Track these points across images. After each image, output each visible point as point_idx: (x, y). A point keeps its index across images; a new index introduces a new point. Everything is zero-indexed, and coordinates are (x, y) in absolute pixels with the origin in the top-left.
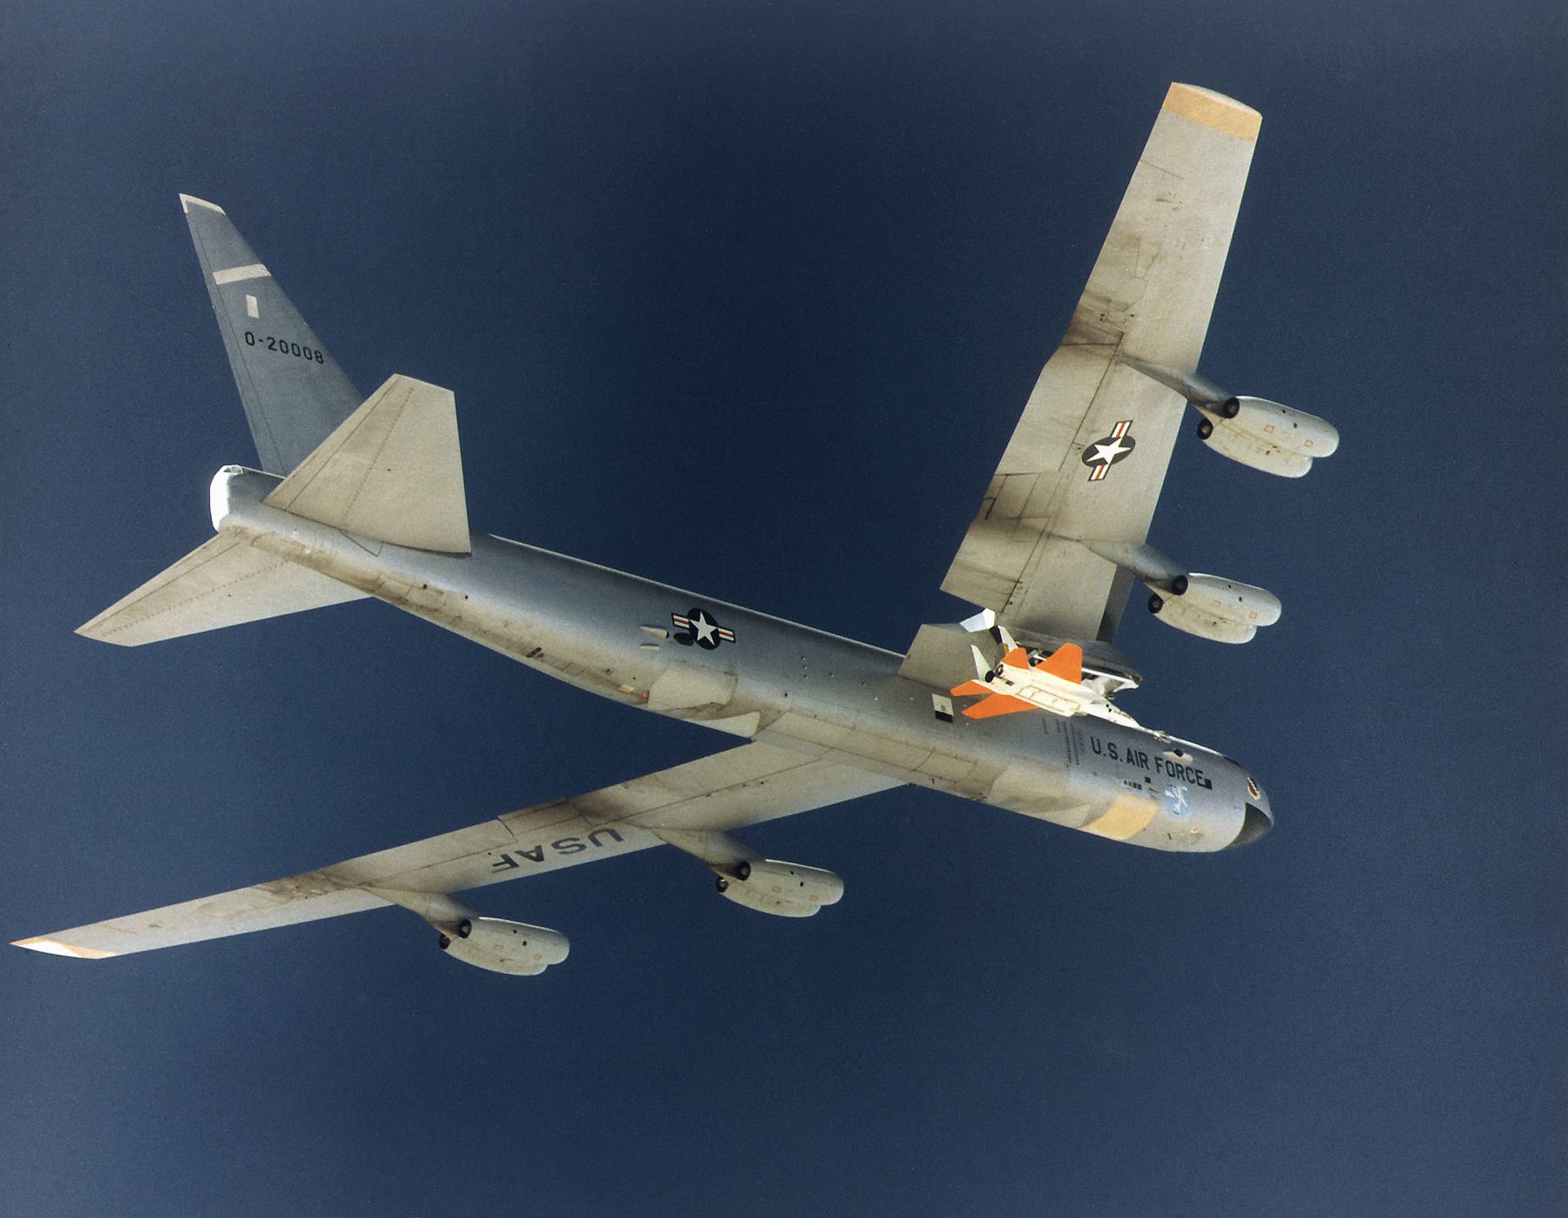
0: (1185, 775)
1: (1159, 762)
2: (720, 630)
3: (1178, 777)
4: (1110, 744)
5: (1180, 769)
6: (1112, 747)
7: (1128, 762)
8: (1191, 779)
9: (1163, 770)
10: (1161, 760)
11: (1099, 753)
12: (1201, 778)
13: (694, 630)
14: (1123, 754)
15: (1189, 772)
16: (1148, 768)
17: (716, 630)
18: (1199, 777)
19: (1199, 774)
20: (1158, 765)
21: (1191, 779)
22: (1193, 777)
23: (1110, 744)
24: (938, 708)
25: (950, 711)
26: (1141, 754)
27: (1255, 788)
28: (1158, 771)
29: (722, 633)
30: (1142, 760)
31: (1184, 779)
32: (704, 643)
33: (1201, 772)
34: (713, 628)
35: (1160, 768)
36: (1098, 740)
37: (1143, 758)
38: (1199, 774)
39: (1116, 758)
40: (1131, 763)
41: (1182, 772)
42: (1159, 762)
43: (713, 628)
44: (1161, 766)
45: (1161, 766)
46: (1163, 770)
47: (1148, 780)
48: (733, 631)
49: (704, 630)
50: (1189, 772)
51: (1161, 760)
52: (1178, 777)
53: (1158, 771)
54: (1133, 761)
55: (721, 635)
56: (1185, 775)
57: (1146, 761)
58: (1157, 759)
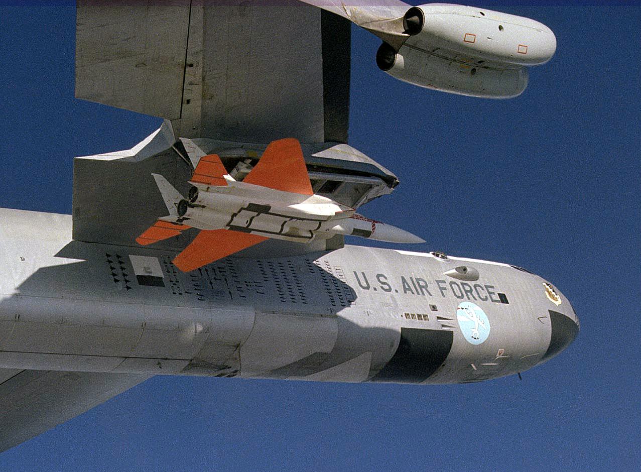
0: (474, 293)
1: (442, 285)
4: (378, 276)
7: (405, 292)
8: (483, 296)
9: (449, 293)
10: (444, 282)
11: (368, 288)
12: (494, 293)
14: (394, 282)
19: (491, 290)
20: (442, 289)
22: (484, 294)
23: (378, 276)
24: (139, 271)
25: (157, 271)
26: (417, 280)
27: (553, 293)
30: (421, 287)
33: (492, 287)
37: (422, 283)
38: (491, 290)
39: (390, 290)
41: (471, 291)
42: (442, 285)
45: (445, 289)
46: (449, 293)
47: (434, 308)
54: (410, 289)
56: (474, 293)
57: (426, 287)
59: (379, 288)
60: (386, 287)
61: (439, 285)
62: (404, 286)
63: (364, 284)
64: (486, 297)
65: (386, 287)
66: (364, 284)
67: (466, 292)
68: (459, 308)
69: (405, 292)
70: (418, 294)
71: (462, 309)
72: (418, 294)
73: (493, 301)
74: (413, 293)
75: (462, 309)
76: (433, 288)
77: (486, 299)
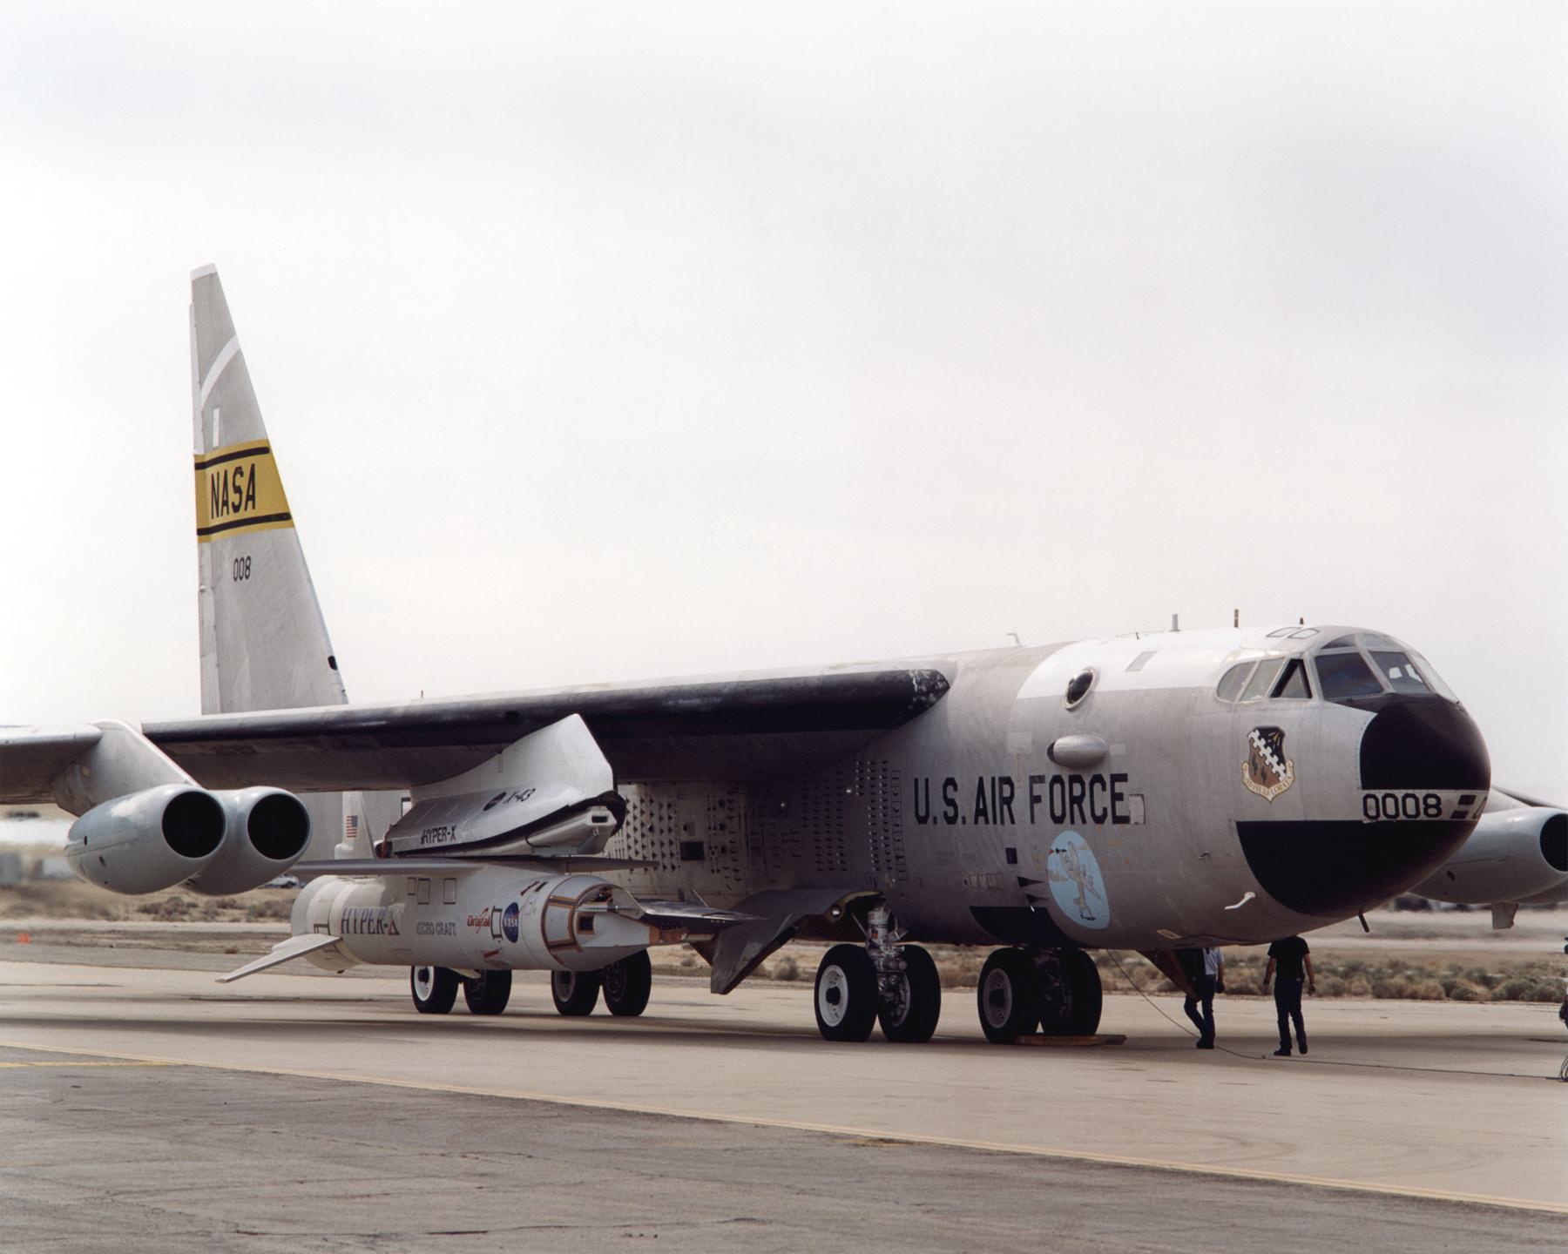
3: (1072, 822)
7: (976, 822)
8: (1099, 812)
10: (1041, 779)
15: (1097, 786)
16: (1013, 822)
18: (1117, 797)
19: (1119, 787)
20: (1036, 799)
21: (1099, 812)
22: (1103, 799)
31: (1084, 821)
33: (1123, 778)
35: (1037, 806)
39: (951, 820)
40: (981, 819)
41: (1077, 800)
46: (1042, 809)
50: (1097, 786)
52: (1072, 822)
57: (1008, 801)
59: (941, 819)
64: (1105, 810)
65: (951, 813)
66: (922, 813)
68: (1051, 852)
69: (976, 822)
70: (995, 822)
72: (995, 822)
74: (987, 821)
75: (1058, 851)
76: (1021, 803)
77: (1099, 820)
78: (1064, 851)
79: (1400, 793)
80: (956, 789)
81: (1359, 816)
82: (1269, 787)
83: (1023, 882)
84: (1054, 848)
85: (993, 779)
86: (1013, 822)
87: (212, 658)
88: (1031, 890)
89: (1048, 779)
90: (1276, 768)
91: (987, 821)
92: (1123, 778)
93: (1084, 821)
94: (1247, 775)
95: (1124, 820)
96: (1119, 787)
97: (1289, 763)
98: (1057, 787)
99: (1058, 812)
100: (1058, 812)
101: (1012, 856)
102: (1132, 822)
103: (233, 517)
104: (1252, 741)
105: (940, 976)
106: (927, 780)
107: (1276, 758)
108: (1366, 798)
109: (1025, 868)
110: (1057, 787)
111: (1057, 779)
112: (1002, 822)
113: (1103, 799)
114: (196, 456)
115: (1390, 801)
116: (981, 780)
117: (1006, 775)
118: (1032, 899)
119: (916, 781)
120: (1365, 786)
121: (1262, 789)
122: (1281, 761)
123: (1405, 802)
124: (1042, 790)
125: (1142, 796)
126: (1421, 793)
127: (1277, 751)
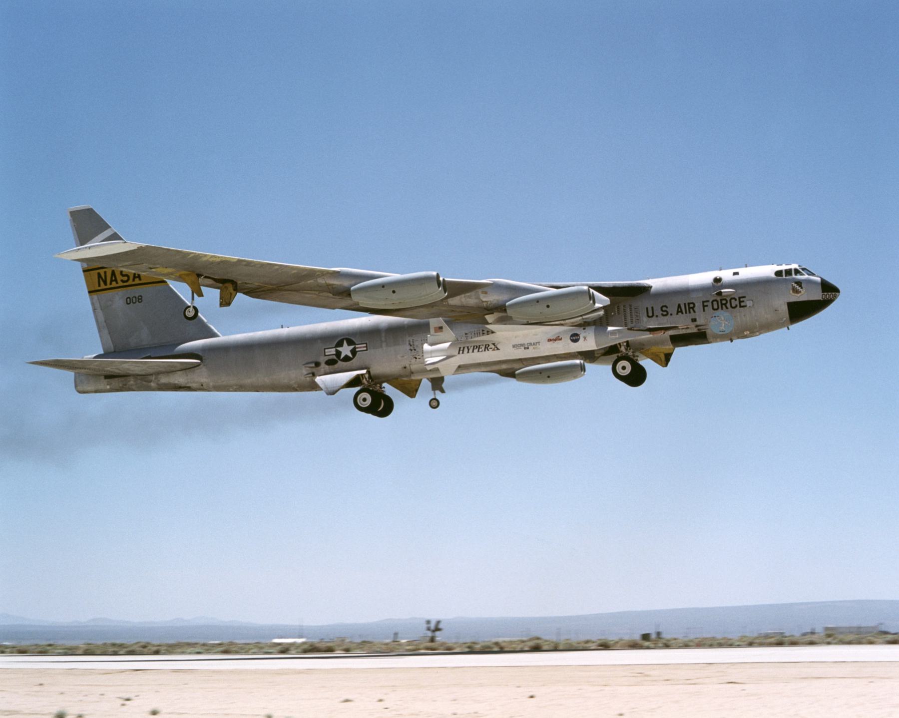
1: (705, 304)
2: (357, 346)
3: (722, 309)
5: (724, 302)
6: (664, 309)
7: (677, 314)
8: (733, 305)
10: (708, 301)
12: (743, 301)
13: (338, 354)
15: (733, 301)
16: (694, 312)
17: (355, 348)
18: (740, 302)
19: (742, 300)
20: (704, 306)
21: (733, 305)
26: (689, 304)
28: (704, 310)
29: (358, 348)
30: (690, 308)
31: (727, 308)
32: (347, 359)
33: (744, 297)
34: (352, 347)
35: (706, 308)
36: (652, 308)
40: (680, 314)
41: (725, 304)
42: (705, 304)
43: (352, 347)
44: (707, 306)
45: (707, 306)
48: (366, 344)
49: (346, 350)
50: (733, 301)
51: (708, 301)
52: (722, 309)
53: (704, 310)
55: (357, 350)
56: (728, 305)
57: (693, 308)
58: (703, 302)
60: (665, 313)
61: (703, 304)
62: (678, 309)
63: (650, 314)
64: (736, 306)
66: (650, 314)
67: (722, 304)
68: (712, 317)
69: (677, 314)
71: (715, 317)
72: (686, 313)
73: (741, 306)
74: (682, 313)
76: (698, 307)
78: (718, 316)
79: (830, 293)
80: (667, 307)
81: (822, 299)
82: (798, 293)
83: (697, 326)
84: (713, 316)
85: (685, 304)
86: (694, 312)
87: (106, 331)
88: (699, 328)
89: (711, 301)
90: (800, 290)
91: (682, 313)
92: (744, 297)
93: (727, 308)
94: (791, 292)
95: (745, 306)
96: (742, 300)
97: (804, 288)
98: (715, 303)
99: (715, 307)
100: (715, 307)
101: (694, 320)
102: (748, 306)
103: (121, 284)
104: (792, 285)
105: (612, 364)
106: (652, 308)
107: (800, 288)
108: (823, 295)
109: (698, 323)
110: (715, 303)
111: (713, 301)
112: (690, 312)
113: (734, 303)
114: (83, 268)
115: (828, 295)
116: (679, 306)
117: (691, 302)
118: (699, 330)
119: (647, 309)
120: (823, 292)
121: (796, 295)
122: (802, 288)
123: (829, 295)
124: (710, 304)
125: (752, 300)
126: (833, 293)
127: (800, 286)
